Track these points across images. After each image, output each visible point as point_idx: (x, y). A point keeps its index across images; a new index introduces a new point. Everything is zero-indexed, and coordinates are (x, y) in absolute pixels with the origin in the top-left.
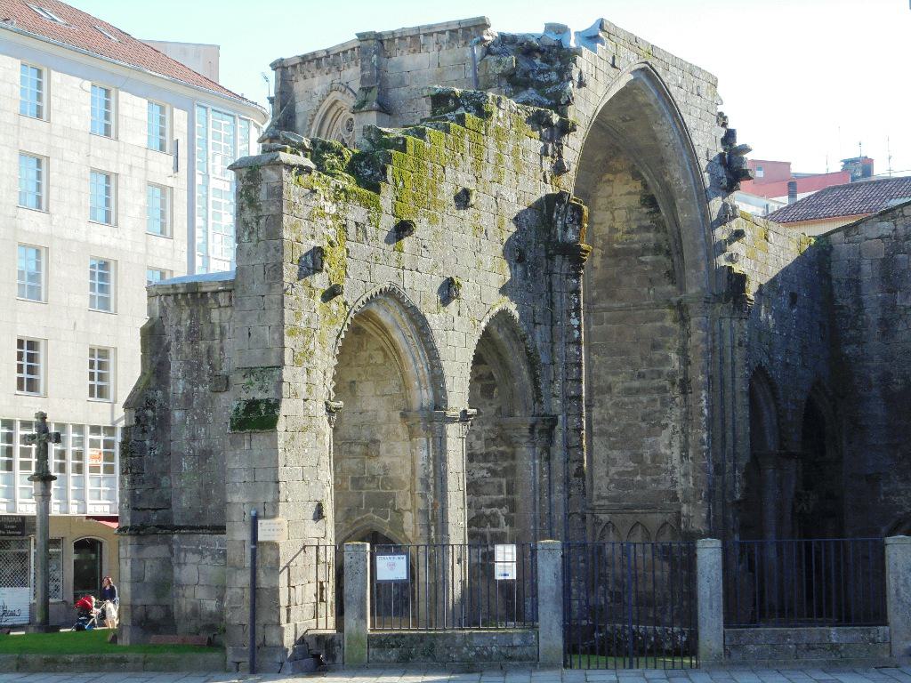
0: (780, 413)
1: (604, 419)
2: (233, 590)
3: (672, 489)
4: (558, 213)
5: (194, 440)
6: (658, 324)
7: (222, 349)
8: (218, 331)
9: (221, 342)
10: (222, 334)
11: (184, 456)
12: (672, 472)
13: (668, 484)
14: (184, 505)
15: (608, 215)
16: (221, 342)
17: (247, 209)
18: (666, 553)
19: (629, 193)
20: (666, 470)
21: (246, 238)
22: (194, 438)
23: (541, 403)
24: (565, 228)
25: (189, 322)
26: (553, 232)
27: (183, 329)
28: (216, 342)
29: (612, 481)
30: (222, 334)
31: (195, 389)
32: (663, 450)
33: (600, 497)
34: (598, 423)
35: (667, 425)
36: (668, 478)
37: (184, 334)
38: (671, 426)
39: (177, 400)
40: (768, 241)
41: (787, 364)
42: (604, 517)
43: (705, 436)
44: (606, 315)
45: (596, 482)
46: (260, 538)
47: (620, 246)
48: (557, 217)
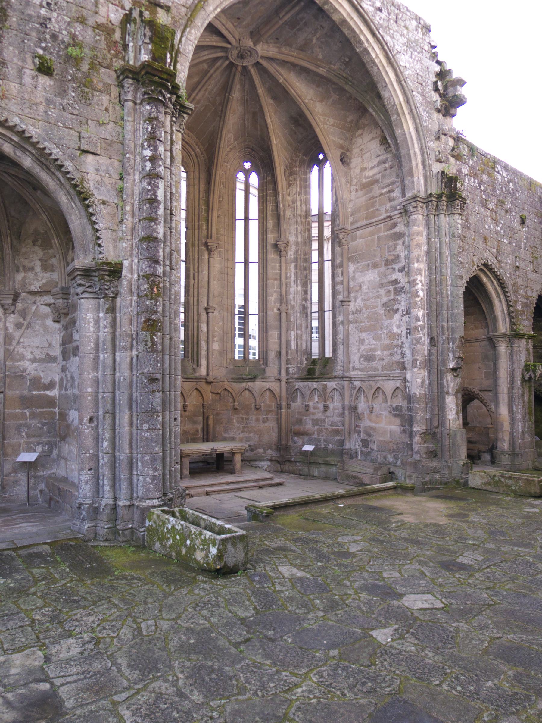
0: (511, 303)
1: (357, 310)
3: (402, 360)
4: (129, 35)
6: (392, 231)
12: (401, 347)
13: (399, 357)
15: (360, 160)
18: (397, 412)
19: (373, 139)
20: (396, 346)
23: (100, 246)
24: (137, 53)
26: (126, 58)
29: (361, 357)
32: (395, 330)
33: (354, 369)
34: (353, 314)
35: (398, 310)
36: (399, 352)
38: (400, 310)
40: (495, 171)
41: (517, 267)
42: (357, 384)
43: (420, 313)
44: (358, 233)
45: (352, 357)
47: (367, 180)
48: (129, 40)
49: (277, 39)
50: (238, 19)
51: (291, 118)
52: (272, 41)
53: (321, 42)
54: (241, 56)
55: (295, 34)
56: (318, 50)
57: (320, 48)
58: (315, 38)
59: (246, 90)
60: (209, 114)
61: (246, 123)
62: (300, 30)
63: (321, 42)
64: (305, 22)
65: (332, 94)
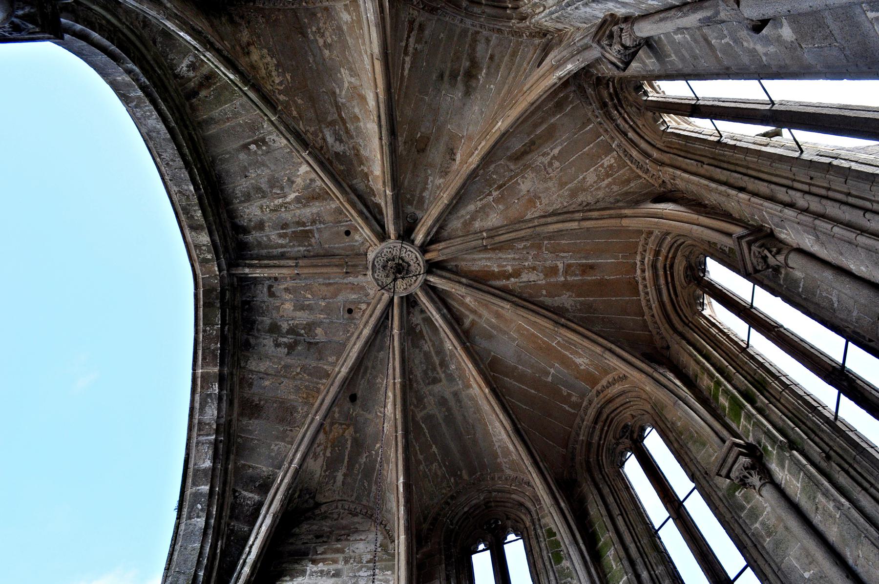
49: (348, 233)
50: (350, 311)
51: (467, 93)
52: (357, 237)
53: (282, 188)
54: (400, 269)
55: (314, 222)
56: (299, 180)
57: (293, 182)
58: (288, 200)
59: (479, 204)
60: (563, 242)
61: (556, 151)
62: (299, 223)
63: (282, 188)
64: (282, 228)
65: (346, 85)
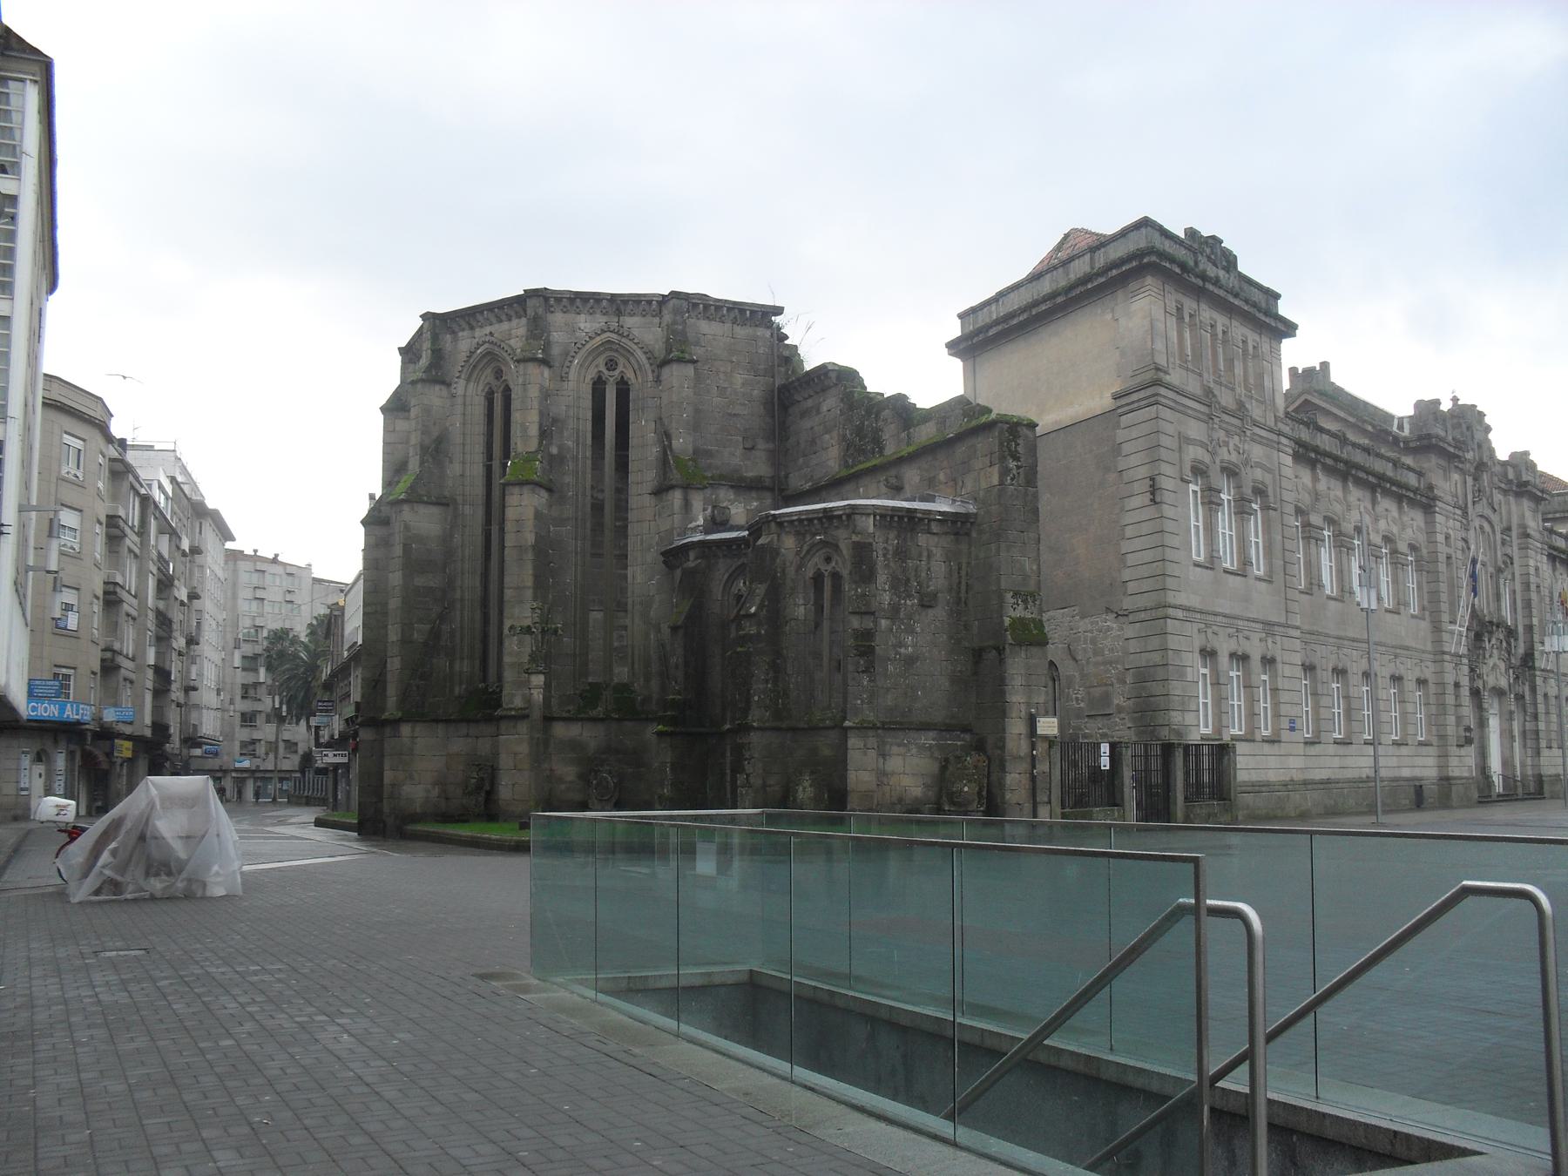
2: (1012, 775)
5: (900, 647)
7: (929, 569)
8: (925, 554)
9: (929, 563)
10: (929, 557)
11: (890, 660)
14: (889, 703)
16: (929, 563)
17: (1008, 457)
21: (1009, 481)
22: (901, 644)
25: (896, 541)
27: (890, 548)
28: (923, 563)
30: (929, 557)
31: (903, 602)
37: (891, 553)
39: (884, 610)
46: (1040, 731)
